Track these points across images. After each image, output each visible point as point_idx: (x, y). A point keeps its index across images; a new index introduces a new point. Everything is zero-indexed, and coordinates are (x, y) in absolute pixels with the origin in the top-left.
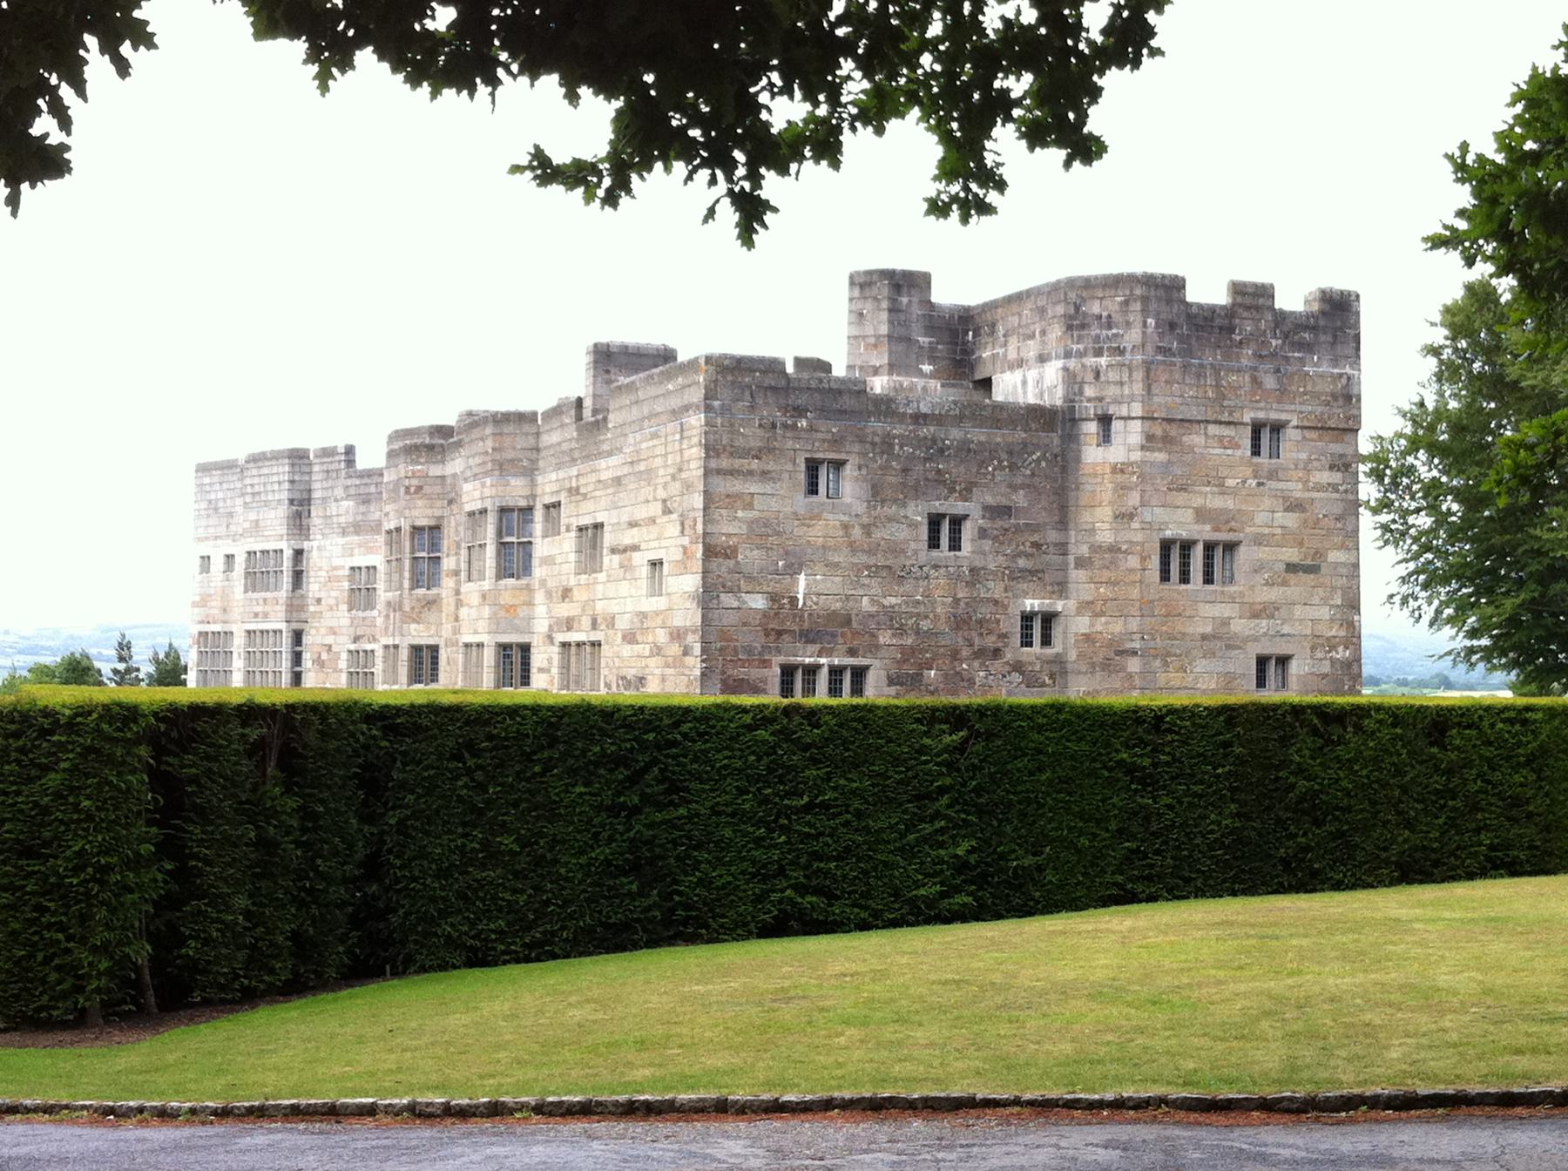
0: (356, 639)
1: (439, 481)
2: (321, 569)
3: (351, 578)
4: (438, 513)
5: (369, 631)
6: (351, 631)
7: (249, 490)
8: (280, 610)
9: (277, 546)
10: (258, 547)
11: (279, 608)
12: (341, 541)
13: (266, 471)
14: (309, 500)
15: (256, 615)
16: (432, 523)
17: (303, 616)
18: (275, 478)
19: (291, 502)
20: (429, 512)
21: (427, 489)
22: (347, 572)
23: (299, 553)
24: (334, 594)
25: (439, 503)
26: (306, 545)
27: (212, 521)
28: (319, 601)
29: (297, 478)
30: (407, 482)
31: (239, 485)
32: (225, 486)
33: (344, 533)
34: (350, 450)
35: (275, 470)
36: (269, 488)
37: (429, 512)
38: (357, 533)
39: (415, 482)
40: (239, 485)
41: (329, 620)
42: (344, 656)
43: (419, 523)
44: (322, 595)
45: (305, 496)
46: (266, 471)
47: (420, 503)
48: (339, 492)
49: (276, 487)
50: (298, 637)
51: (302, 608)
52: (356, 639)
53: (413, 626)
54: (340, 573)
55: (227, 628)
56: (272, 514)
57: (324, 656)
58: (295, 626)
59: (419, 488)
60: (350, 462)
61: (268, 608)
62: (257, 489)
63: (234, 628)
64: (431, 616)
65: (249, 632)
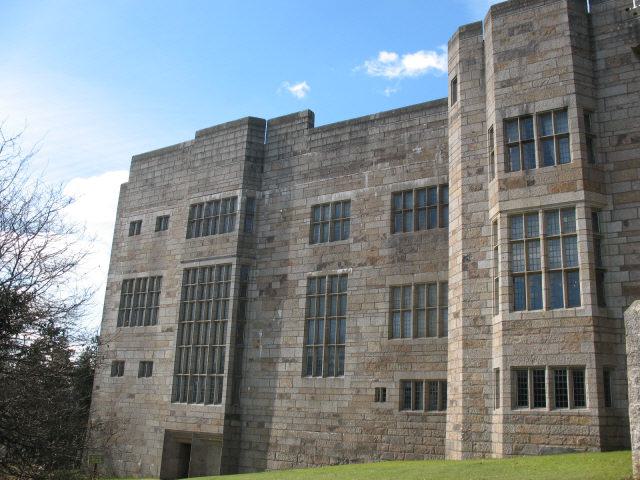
2: (274, 212)
3: (313, 217)
6: (316, 260)
8: (232, 248)
9: (230, 194)
10: (205, 199)
14: (263, 159)
15: (201, 254)
18: (232, 142)
22: (309, 210)
23: (249, 202)
26: (258, 194)
27: (146, 195)
28: (270, 239)
32: (162, 167)
34: (311, 115)
35: (232, 136)
38: (323, 176)
42: (304, 283)
45: (259, 155)
46: (216, 140)
49: (232, 149)
51: (252, 246)
55: (156, 273)
58: (243, 260)
60: (311, 125)
63: (164, 273)
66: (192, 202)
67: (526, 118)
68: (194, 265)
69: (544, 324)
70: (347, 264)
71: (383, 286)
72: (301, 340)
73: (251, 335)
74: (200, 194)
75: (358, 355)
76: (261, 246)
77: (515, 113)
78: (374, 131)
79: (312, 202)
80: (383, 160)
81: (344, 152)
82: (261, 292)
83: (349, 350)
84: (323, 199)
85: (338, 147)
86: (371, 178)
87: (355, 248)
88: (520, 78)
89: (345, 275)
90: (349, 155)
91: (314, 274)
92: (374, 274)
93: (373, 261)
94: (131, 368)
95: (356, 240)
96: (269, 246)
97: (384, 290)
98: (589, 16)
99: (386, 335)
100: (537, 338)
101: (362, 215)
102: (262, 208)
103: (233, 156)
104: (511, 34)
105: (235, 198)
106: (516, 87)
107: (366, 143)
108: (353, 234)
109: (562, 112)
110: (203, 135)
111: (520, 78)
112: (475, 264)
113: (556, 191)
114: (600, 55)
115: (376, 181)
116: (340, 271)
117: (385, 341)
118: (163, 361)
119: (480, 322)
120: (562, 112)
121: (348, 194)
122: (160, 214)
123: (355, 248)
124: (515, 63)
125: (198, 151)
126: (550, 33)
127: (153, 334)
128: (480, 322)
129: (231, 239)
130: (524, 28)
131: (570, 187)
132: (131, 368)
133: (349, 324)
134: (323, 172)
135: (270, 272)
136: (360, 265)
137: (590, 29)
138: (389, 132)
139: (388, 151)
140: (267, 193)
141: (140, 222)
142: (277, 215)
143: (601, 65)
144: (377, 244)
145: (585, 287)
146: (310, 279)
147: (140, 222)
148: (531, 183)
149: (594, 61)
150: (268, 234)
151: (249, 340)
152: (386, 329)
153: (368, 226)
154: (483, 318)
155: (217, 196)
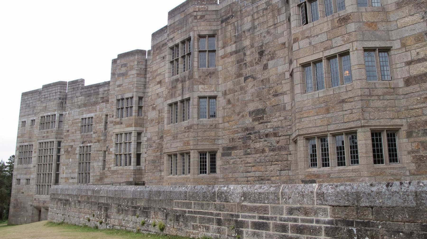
0: (83, 143)
1: (214, 13)
2: (69, 120)
3: (81, 122)
4: (214, 28)
5: (89, 139)
6: (82, 140)
7: (43, 97)
8: (54, 135)
9: (53, 113)
10: (45, 115)
11: (53, 134)
12: (78, 110)
13: (50, 90)
15: (44, 137)
16: (211, 33)
17: (62, 136)
18: (54, 92)
19: (60, 98)
20: (209, 28)
21: (207, 17)
22: (80, 120)
23: (61, 115)
24: (74, 128)
25: (215, 24)
26: (64, 113)
27: (27, 110)
28: (68, 131)
29: (62, 91)
30: (195, 14)
31: (38, 97)
32: (33, 98)
33: (80, 107)
34: (83, 81)
35: (54, 89)
36: (51, 95)
37: (209, 28)
39: (200, 13)
40: (38, 97)
41: (72, 137)
42: (78, 149)
43: (202, 33)
44: (70, 129)
45: (65, 97)
46: (50, 90)
47: (203, 23)
48: (78, 94)
49: (54, 94)
50: (59, 143)
51: (61, 134)
52: (83, 143)
53: (200, 87)
54: (78, 121)
55: (31, 143)
56: (52, 103)
57: (70, 149)
58: (59, 140)
59: (202, 17)
61: (48, 134)
62: (46, 96)
63: (33, 143)
64: (212, 81)
65: (40, 143)
66: (41, 115)
67: (123, 99)
68: (42, 141)
69: (121, 171)
70: (91, 142)
71: (101, 151)
72: (77, 170)
73: (62, 168)
74: (44, 112)
75: (94, 176)
76: (65, 134)
77: (120, 97)
78: (101, 90)
79: (81, 117)
80: (103, 102)
81: (92, 98)
82: (65, 152)
83: (91, 174)
84: (85, 116)
85: (89, 96)
86: (99, 108)
87: (94, 136)
88: (122, 84)
89: (90, 146)
90: (93, 99)
91: (81, 145)
92: (99, 146)
93: (99, 141)
94: (23, 181)
95: (94, 133)
96: (68, 134)
97: (101, 152)
98: (146, 61)
99: (102, 169)
100: (119, 176)
101: (97, 123)
102: (66, 118)
103: (54, 97)
104: (122, 67)
105: (55, 115)
106: (121, 88)
107: (98, 94)
108: (93, 131)
109: (132, 98)
110: (46, 87)
111: (122, 84)
112: (109, 149)
113: (128, 127)
114: (148, 76)
115: (101, 110)
116: (89, 145)
117: (101, 171)
118: (33, 179)
119: (110, 170)
120: (132, 98)
121: (92, 115)
122: (32, 119)
123: (94, 136)
124: (121, 78)
125: (43, 94)
126: (132, 68)
127: (29, 168)
128: (110, 170)
129: (54, 131)
130: (125, 65)
131: (130, 126)
132: (23, 181)
133: (91, 164)
134: (85, 105)
135: (67, 144)
136: (95, 142)
137: (146, 65)
138: (105, 91)
139: (105, 98)
140: (67, 112)
141: (25, 122)
142: (70, 122)
143: (148, 80)
144: (100, 135)
145: (133, 160)
146: (81, 147)
147: (25, 122)
148: (121, 123)
149: (146, 78)
150: (67, 129)
151: (61, 170)
152: (102, 167)
153: (98, 127)
154: (110, 168)
155: (49, 114)
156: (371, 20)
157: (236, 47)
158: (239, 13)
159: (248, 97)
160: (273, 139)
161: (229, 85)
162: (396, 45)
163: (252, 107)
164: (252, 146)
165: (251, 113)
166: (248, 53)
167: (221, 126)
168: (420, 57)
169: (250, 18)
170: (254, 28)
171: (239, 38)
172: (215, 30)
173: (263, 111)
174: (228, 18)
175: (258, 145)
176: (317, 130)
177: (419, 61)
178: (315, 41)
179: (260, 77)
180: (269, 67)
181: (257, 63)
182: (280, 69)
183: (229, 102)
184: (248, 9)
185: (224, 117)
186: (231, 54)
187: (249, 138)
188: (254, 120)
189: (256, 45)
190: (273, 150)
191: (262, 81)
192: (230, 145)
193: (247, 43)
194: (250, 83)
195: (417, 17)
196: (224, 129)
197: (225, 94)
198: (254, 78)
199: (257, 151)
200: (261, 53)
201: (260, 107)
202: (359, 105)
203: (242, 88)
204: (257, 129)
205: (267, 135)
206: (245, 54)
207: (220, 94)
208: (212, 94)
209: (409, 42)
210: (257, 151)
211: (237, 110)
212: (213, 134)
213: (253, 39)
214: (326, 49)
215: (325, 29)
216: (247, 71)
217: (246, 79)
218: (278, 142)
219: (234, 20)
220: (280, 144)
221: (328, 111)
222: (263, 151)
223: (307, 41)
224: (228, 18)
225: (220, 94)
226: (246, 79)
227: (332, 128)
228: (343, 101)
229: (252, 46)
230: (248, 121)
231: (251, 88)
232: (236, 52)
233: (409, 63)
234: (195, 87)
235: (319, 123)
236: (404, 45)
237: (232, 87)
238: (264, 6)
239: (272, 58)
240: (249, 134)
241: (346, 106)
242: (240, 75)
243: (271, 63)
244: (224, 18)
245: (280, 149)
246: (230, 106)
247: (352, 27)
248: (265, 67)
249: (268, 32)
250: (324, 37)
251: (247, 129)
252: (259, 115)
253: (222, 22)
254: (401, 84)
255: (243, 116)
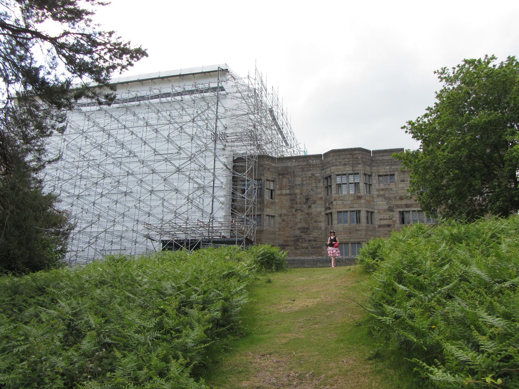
4: (274, 177)
16: (273, 179)
21: (271, 169)
37: (272, 176)
39: (267, 166)
47: (269, 173)
59: (268, 169)
156: (368, 199)
157: (290, 192)
158: (292, 174)
159: (298, 220)
160: (314, 243)
161: (284, 211)
162: (376, 211)
163: (300, 225)
164: (300, 245)
165: (299, 229)
166: (298, 197)
167: (277, 233)
168: (385, 218)
169: (300, 179)
170: (302, 185)
171: (292, 188)
172: (275, 178)
173: (308, 229)
174: (284, 174)
175: (304, 245)
176: (345, 241)
177: (384, 219)
178: (345, 203)
179: (306, 211)
180: (312, 207)
181: (304, 204)
182: (319, 210)
183: (284, 220)
184: (299, 174)
185: (279, 228)
186: (286, 195)
187: (299, 241)
188: (301, 232)
189: (304, 194)
190: (313, 248)
191: (307, 213)
192: (285, 244)
193: (298, 191)
194: (299, 213)
195: (384, 203)
196: (280, 235)
197: (280, 216)
198: (302, 211)
199: (303, 248)
200: (307, 199)
201: (306, 226)
202: (365, 233)
203: (293, 215)
204: (303, 237)
205: (310, 241)
206: (296, 197)
207: (277, 215)
208: (273, 215)
209: (381, 212)
210: (303, 248)
211: (290, 226)
212: (273, 236)
213: (302, 190)
214: (350, 207)
215: (351, 199)
216: (298, 206)
217: (296, 210)
218: (316, 244)
219: (288, 176)
220: (317, 245)
221: (350, 233)
222: (307, 248)
223: (341, 202)
224: (284, 174)
225: (277, 215)
226: (296, 210)
227: (352, 240)
228: (358, 230)
229: (301, 194)
230: (298, 232)
231: (299, 216)
232: (290, 195)
233: (380, 219)
234: (265, 209)
235: (346, 238)
236: (379, 212)
237: (286, 213)
238: (310, 175)
239: (314, 203)
240: (297, 239)
241: (359, 232)
242: (292, 208)
243: (313, 206)
244: (281, 173)
245: (317, 248)
246: (284, 223)
247: (363, 201)
248: (310, 207)
249: (312, 190)
250: (350, 202)
251: (297, 236)
252: (305, 230)
253: (279, 175)
254: (377, 227)
255: (294, 229)
